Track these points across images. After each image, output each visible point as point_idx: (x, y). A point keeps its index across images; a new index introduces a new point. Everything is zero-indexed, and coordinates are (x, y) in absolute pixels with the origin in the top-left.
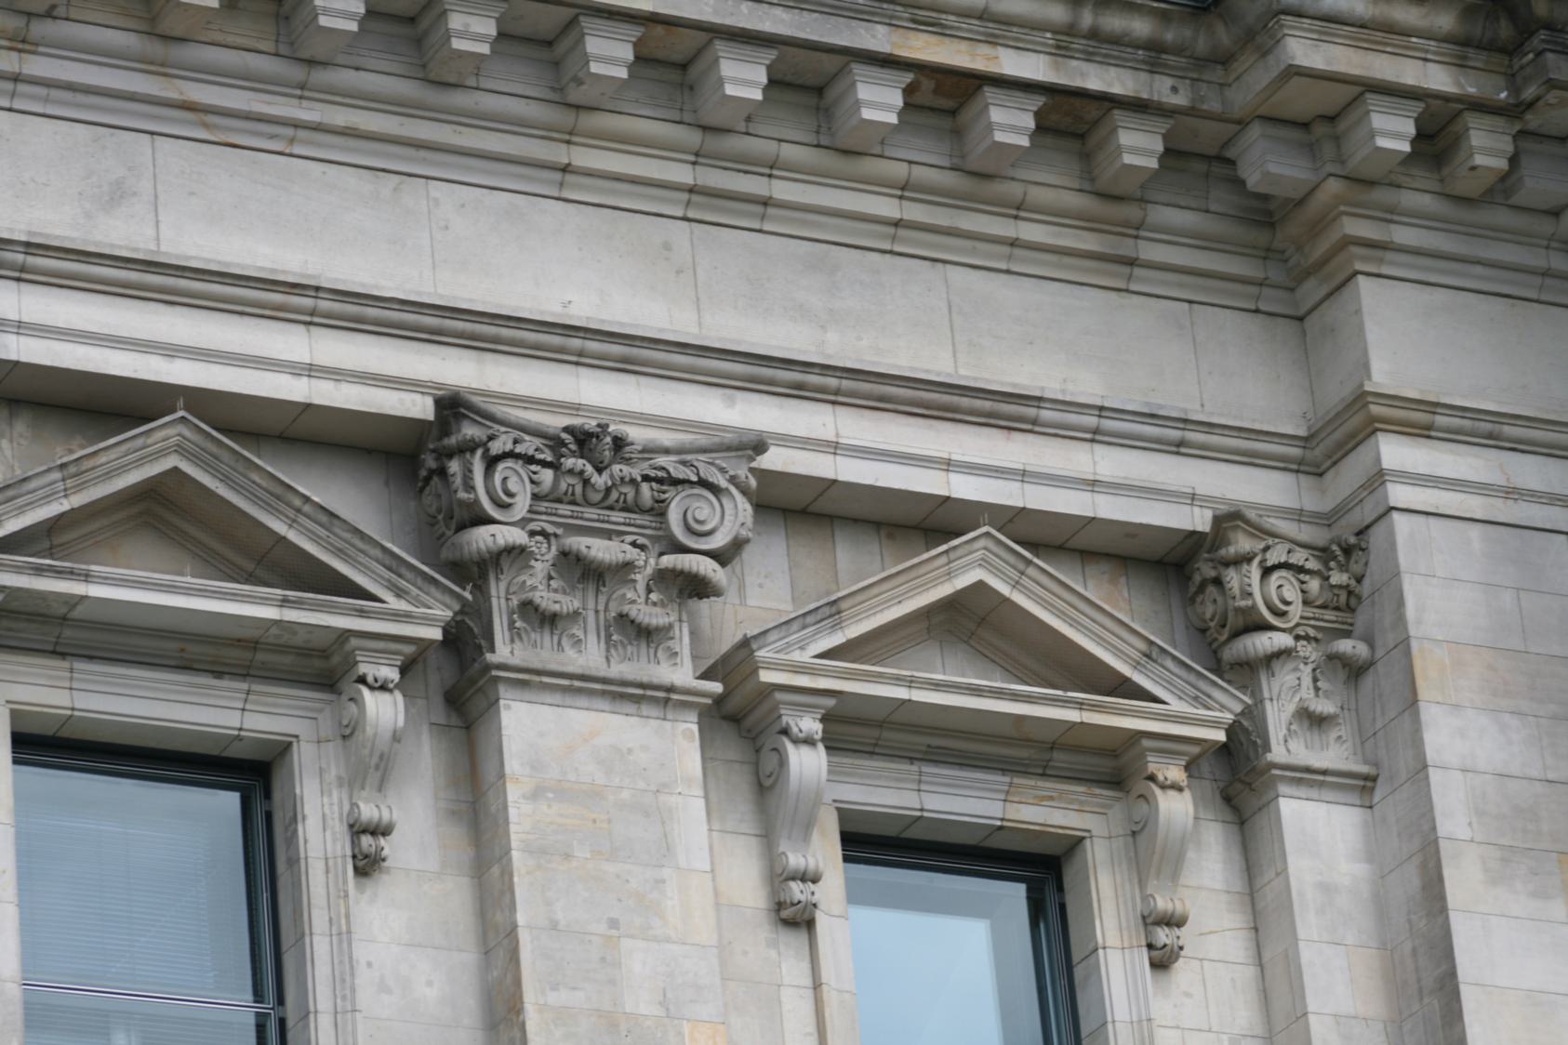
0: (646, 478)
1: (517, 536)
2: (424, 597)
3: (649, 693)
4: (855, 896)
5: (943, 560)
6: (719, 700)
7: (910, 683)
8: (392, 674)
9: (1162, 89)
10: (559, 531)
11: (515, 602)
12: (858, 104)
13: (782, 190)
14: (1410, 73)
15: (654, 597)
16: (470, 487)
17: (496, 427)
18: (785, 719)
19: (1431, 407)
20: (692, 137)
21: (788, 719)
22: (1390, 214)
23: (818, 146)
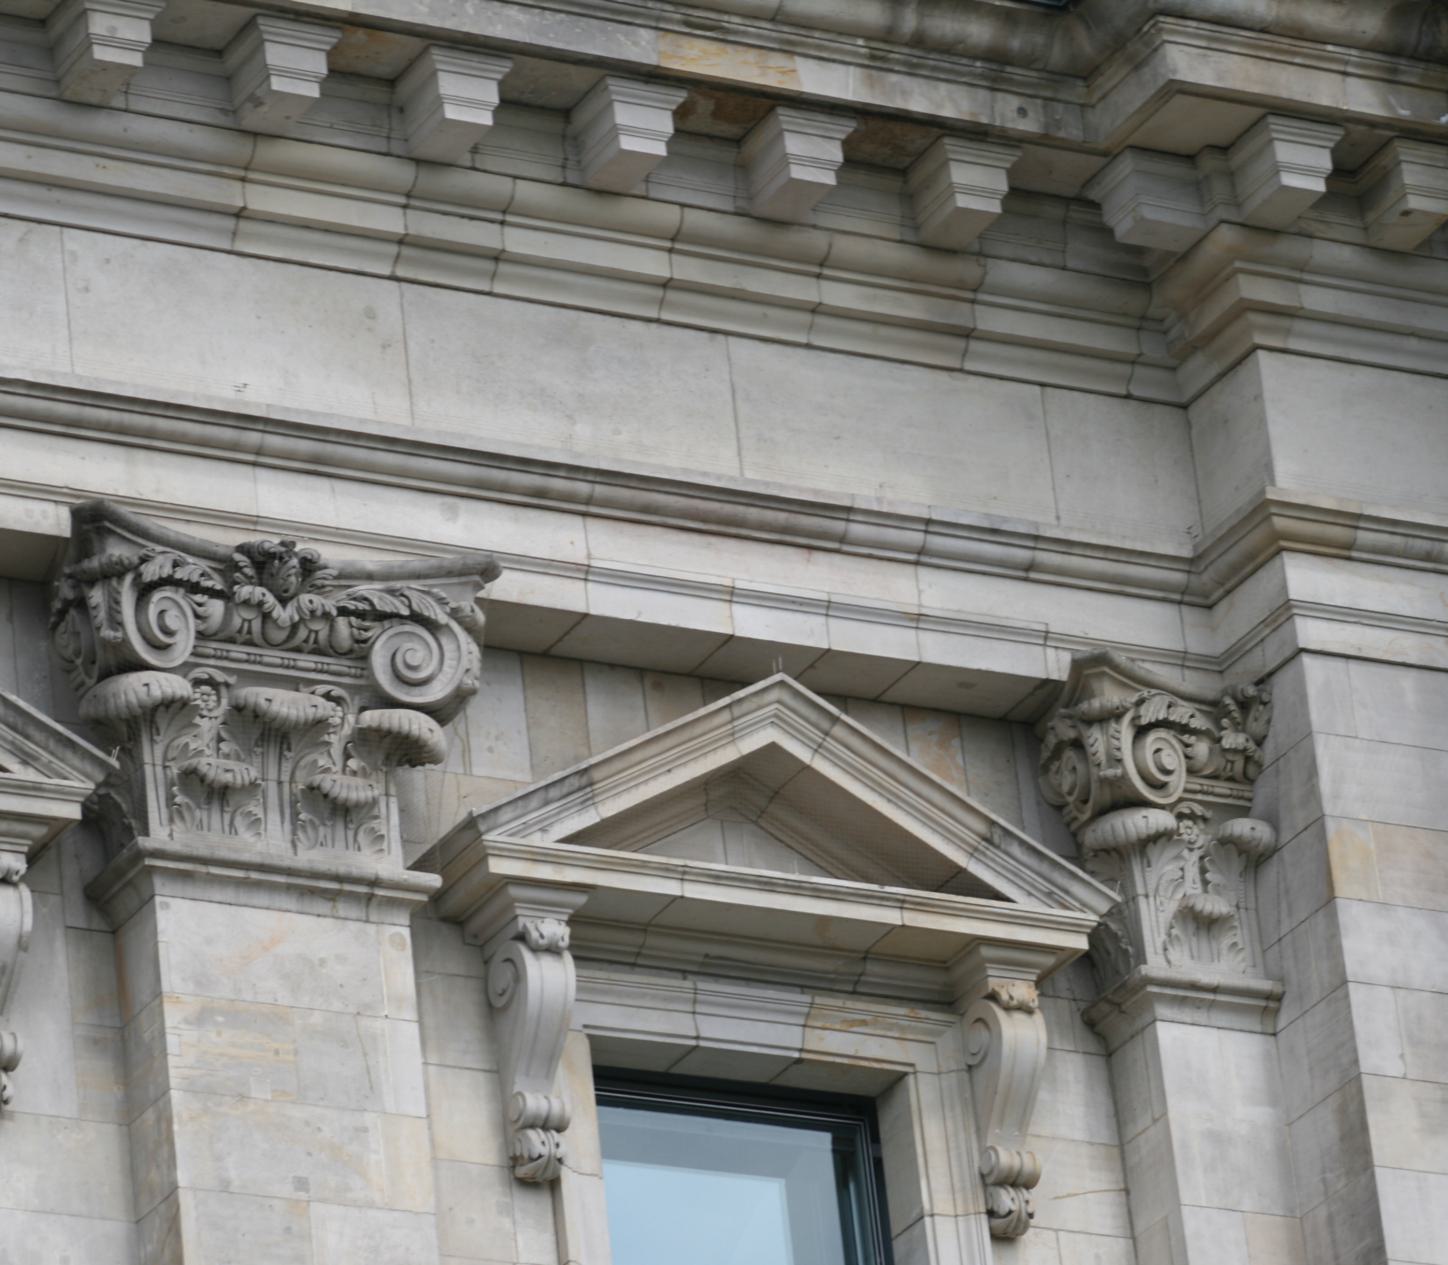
0: (343, 611)
1: (176, 686)
2: (57, 764)
3: (347, 887)
4: (612, 1148)
5: (725, 716)
6: (437, 897)
7: (683, 874)
8: (18, 864)
9: (1006, 111)
10: (232, 680)
11: (175, 771)
12: (615, 131)
13: (518, 241)
14: (1324, 90)
15: (353, 764)
16: (116, 623)
17: (151, 545)
18: (521, 921)
19: (1355, 520)
20: (402, 173)
21: (526, 921)
22: (1300, 272)
23: (564, 184)
